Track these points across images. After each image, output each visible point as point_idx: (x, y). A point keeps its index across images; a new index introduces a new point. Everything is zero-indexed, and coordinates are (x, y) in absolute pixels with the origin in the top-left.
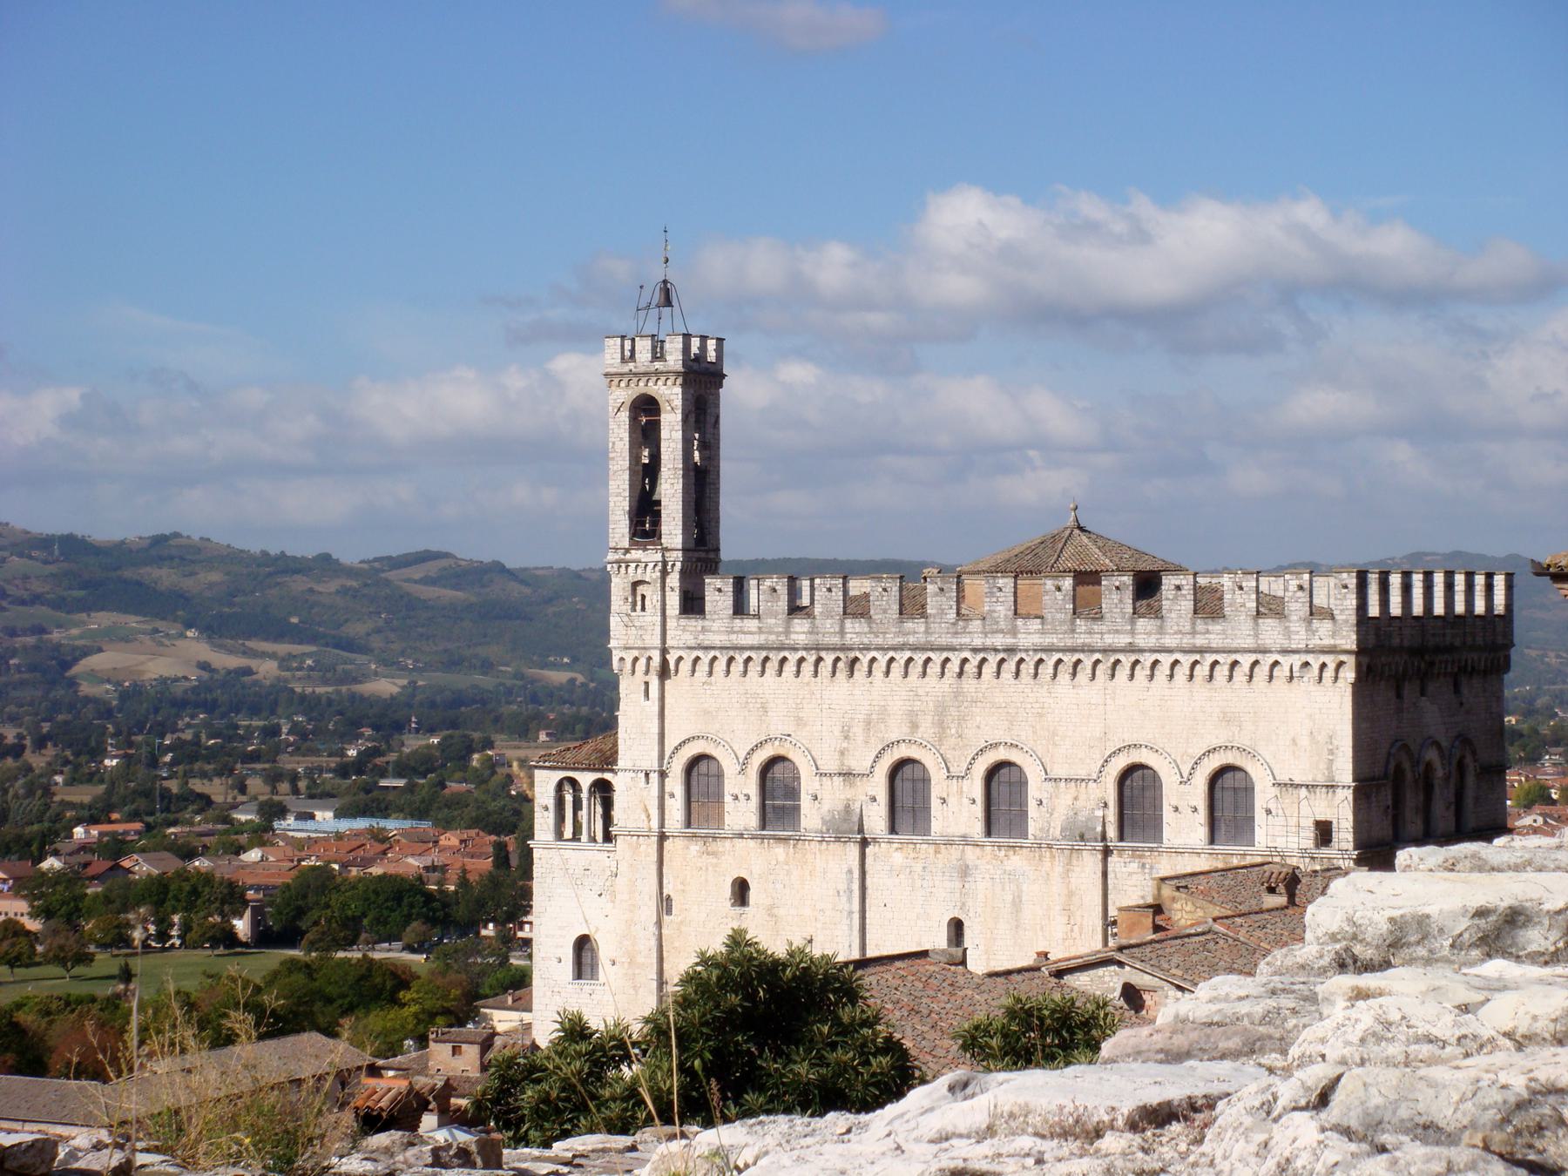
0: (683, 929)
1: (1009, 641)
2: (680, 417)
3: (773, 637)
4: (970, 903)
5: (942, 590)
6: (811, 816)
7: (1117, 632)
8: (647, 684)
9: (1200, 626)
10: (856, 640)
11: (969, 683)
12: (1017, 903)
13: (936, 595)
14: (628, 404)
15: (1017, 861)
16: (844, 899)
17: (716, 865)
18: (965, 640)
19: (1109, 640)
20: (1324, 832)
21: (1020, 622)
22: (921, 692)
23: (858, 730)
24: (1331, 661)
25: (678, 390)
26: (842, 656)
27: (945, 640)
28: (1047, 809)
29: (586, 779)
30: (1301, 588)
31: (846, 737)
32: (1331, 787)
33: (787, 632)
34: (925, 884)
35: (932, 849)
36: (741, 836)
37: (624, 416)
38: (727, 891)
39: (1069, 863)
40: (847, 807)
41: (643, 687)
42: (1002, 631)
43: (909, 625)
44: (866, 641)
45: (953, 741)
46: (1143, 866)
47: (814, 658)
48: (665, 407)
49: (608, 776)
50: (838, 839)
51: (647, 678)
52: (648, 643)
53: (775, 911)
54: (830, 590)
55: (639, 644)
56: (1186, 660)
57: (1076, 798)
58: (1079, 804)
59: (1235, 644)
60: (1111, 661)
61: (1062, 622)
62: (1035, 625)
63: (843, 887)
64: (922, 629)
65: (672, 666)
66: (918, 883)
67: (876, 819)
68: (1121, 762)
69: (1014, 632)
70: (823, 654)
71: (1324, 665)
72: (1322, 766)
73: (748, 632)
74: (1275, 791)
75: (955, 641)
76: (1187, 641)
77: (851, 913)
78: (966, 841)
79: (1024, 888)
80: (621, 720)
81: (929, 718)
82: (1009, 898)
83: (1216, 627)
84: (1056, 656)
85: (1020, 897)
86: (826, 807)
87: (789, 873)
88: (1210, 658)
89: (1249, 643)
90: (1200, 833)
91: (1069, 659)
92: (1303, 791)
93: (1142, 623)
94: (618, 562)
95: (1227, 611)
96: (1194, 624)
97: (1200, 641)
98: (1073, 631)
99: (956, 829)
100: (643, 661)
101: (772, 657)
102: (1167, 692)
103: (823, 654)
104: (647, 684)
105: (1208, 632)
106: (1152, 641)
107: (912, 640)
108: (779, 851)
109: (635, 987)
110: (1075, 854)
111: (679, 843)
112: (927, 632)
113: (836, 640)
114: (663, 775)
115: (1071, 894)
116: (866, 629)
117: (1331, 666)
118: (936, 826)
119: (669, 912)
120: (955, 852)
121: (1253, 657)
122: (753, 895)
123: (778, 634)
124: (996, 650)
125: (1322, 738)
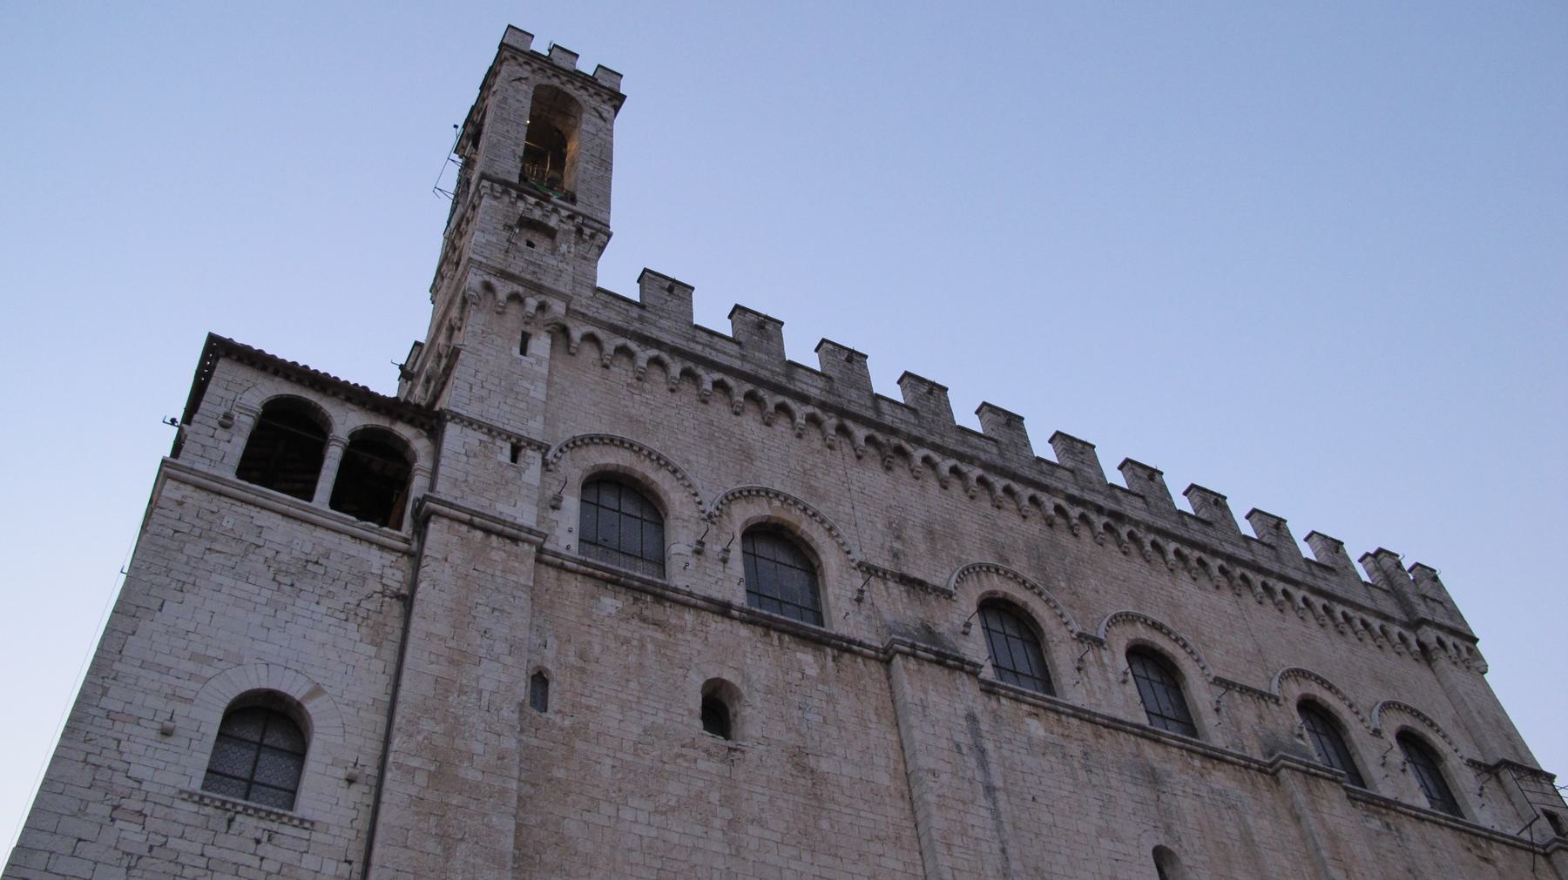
0: (579, 745)
11: (1065, 539)
16: (972, 762)
22: (1000, 523)
26: (880, 437)
29: (345, 422)
31: (898, 538)
36: (724, 609)
49: (403, 431)
51: (528, 329)
52: (547, 281)
53: (812, 761)
63: (964, 739)
70: (849, 424)
100: (532, 303)
108: (806, 658)
109: (447, 841)
111: (574, 586)
123: (773, 372)
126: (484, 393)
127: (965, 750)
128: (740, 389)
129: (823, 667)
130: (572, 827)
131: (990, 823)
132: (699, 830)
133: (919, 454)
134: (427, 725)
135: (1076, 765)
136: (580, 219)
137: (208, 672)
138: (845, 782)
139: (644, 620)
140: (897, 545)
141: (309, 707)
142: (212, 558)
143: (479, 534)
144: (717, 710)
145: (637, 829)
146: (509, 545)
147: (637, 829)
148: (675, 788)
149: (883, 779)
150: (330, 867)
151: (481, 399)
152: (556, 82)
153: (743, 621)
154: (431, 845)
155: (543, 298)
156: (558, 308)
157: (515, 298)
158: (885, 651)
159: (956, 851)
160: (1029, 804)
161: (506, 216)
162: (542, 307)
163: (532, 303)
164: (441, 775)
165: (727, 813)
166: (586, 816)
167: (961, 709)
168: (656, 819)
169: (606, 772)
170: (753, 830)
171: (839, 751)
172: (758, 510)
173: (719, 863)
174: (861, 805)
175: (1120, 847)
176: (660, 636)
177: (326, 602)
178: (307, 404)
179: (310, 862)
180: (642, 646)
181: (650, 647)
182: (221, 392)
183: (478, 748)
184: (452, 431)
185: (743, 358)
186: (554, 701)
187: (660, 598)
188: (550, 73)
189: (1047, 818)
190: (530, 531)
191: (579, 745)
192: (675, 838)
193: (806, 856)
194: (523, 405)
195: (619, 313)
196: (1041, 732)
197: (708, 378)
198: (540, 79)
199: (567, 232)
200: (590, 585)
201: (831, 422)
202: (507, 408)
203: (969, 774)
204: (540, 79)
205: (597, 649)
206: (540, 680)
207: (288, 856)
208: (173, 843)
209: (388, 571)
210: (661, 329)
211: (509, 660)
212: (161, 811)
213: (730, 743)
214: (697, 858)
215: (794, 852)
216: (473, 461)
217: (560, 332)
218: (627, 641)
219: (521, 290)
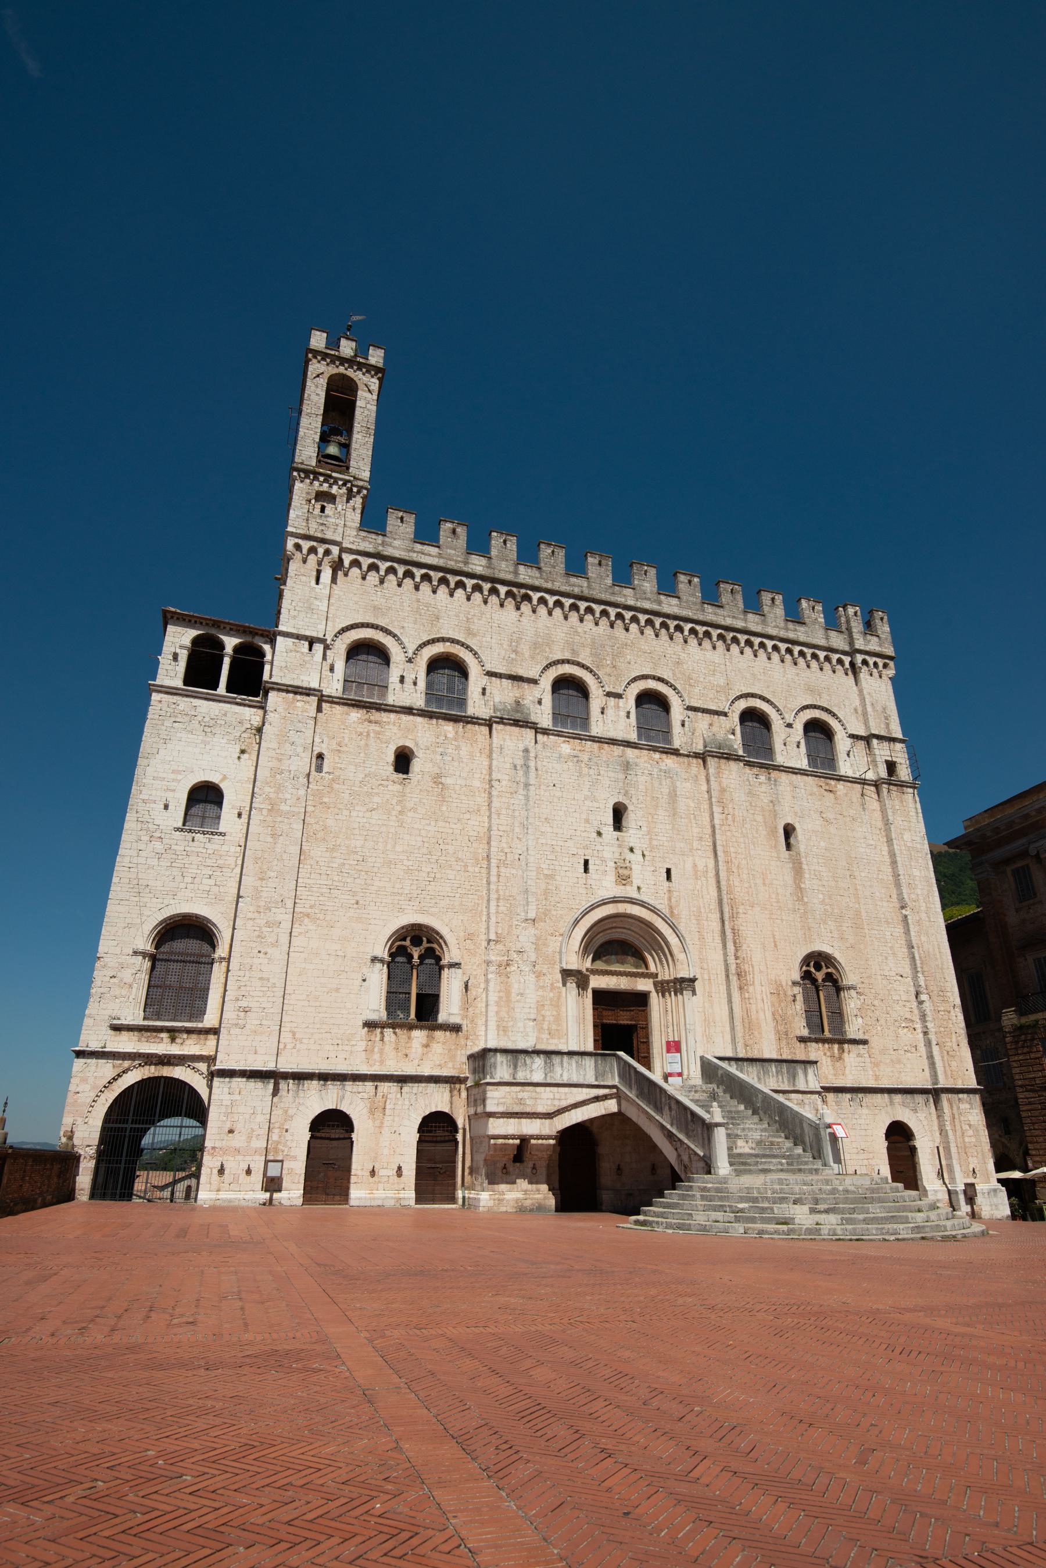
0: (336, 786)
1: (655, 607)
2: (375, 397)
3: (453, 563)
4: (632, 791)
5: (600, 564)
6: (476, 706)
7: (734, 617)
8: (319, 572)
9: (791, 625)
10: (529, 581)
12: (673, 796)
13: (593, 565)
14: (327, 376)
15: (670, 761)
16: (521, 773)
17: (378, 733)
18: (620, 600)
19: (729, 622)
20: (891, 766)
21: (662, 597)
22: (580, 630)
23: (525, 649)
24: (880, 662)
25: (375, 381)
26: (515, 590)
27: (603, 596)
28: (687, 731)
29: (230, 643)
30: (856, 614)
32: (894, 740)
33: (466, 563)
34: (592, 772)
35: (596, 745)
36: (409, 711)
37: (323, 382)
38: (391, 758)
39: (719, 767)
40: (518, 703)
41: (315, 573)
42: (649, 599)
43: (573, 580)
44: (537, 583)
45: (608, 670)
46: (769, 779)
47: (489, 585)
48: (361, 386)
50: (516, 723)
52: (329, 536)
53: (443, 780)
54: (505, 542)
55: (319, 535)
56: (783, 646)
57: (711, 725)
58: (715, 729)
59: (816, 641)
60: (729, 636)
61: (695, 604)
62: (674, 601)
63: (519, 762)
64: (585, 584)
65: (346, 563)
66: (585, 770)
67: (544, 717)
68: (743, 705)
69: (660, 603)
70: (499, 586)
71: (875, 664)
72: (883, 726)
73: (429, 555)
74: (849, 741)
75: (613, 599)
76: (783, 634)
77: (527, 785)
78: (628, 744)
79: (678, 784)
80: (287, 594)
81: (588, 650)
82: (666, 791)
83: (802, 629)
84: (690, 625)
85: (675, 791)
86: (497, 700)
87: (458, 748)
88: (796, 649)
89: (822, 642)
90: (803, 763)
91: (701, 629)
92: (875, 741)
93: (750, 616)
94: (307, 473)
95: (807, 620)
96: (786, 625)
97: (791, 635)
98: (703, 611)
99: (620, 735)
100: (321, 551)
101: (448, 578)
102: (769, 665)
103: (499, 586)
104: (319, 572)
105: (796, 630)
106: (758, 629)
107: (576, 591)
108: (449, 728)
110: (723, 761)
111: (338, 709)
112: (589, 587)
113: (509, 577)
114: (327, 648)
115: (723, 790)
116: (538, 575)
117: (881, 665)
118: (596, 730)
119: (319, 769)
120: (617, 750)
121: (825, 653)
122: (416, 765)
123: (457, 561)
124: (645, 611)
125: (879, 708)
126: (296, 613)
127: (518, 768)
128: (436, 576)
129: (457, 733)
130: (330, 822)
131: (523, 802)
132: (385, 817)
133: (536, 596)
134: (267, 789)
135: (583, 765)
136: (349, 485)
137: (180, 777)
138: (457, 788)
139: (370, 722)
140: (513, 656)
141: (222, 786)
142: (175, 725)
143: (291, 695)
144: (403, 761)
145: (358, 820)
146: (306, 698)
147: (358, 820)
148: (376, 799)
149: (477, 783)
150: (233, 849)
151: (295, 617)
152: (341, 369)
153: (419, 715)
154: (269, 839)
155: (327, 546)
156: (335, 550)
157: (313, 550)
158: (490, 720)
159: (502, 817)
160: (551, 788)
161: (308, 493)
162: (327, 552)
163: (321, 551)
164: (273, 809)
165: (399, 808)
166: (337, 817)
167: (521, 747)
168: (368, 814)
169: (346, 796)
170: (410, 814)
171: (457, 773)
172: (439, 648)
173: (392, 830)
174: (463, 797)
175: (596, 805)
176: (378, 729)
177: (226, 737)
178: (213, 635)
179: (225, 848)
180: (368, 735)
181: (372, 735)
182: (172, 639)
183: (288, 796)
184: (279, 639)
185: (440, 556)
186: (325, 768)
187: (379, 708)
188: (337, 363)
189: (559, 794)
190: (314, 690)
191: (336, 786)
192: (373, 822)
193: (433, 823)
194: (315, 616)
195: (370, 543)
196: (568, 751)
197: (418, 573)
198: (333, 370)
199: (342, 496)
200: (346, 708)
201: (486, 586)
202: (307, 620)
203: (518, 779)
204: (333, 370)
205: (347, 739)
206: (320, 756)
207: (216, 847)
208: (174, 847)
209: (253, 717)
210: (394, 548)
211: (303, 755)
212: (168, 836)
213: (405, 776)
214: (384, 829)
215: (428, 822)
216: (290, 654)
217: (337, 566)
218: (361, 734)
219: (315, 544)
